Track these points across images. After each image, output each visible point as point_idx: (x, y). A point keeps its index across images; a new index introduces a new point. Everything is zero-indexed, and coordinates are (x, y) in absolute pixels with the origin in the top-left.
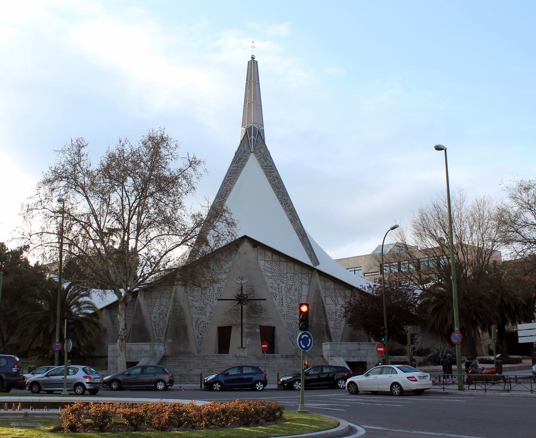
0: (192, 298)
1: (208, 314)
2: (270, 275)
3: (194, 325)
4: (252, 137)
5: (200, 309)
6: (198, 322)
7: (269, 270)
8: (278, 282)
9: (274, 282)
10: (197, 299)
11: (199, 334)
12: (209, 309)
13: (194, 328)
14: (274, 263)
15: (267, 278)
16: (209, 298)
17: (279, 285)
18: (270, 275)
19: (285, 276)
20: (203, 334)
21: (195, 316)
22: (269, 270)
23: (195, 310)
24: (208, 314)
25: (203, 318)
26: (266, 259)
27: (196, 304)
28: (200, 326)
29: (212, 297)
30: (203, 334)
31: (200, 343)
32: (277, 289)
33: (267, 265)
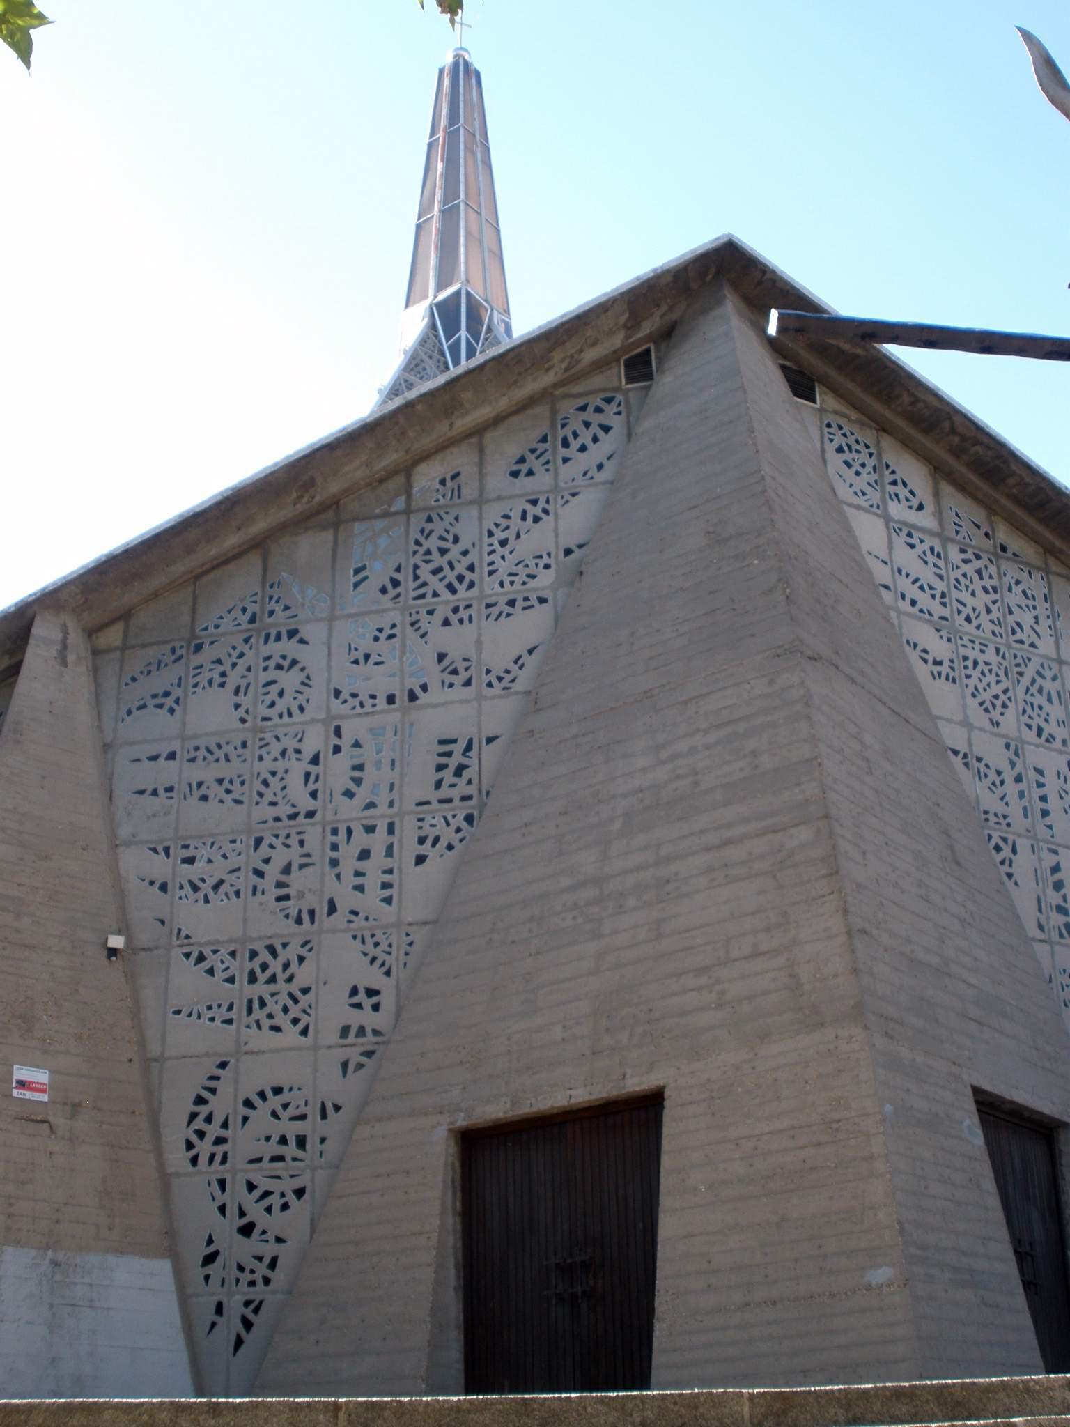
0: (160, 867)
1: (331, 1010)
2: (939, 648)
3: (176, 1132)
4: (463, 333)
5: (240, 967)
6: (220, 1105)
7: (924, 600)
8: (1010, 721)
9: (979, 718)
10: (219, 870)
11: (225, 1229)
12: (338, 962)
13: (177, 1158)
14: (954, 555)
15: (922, 672)
16: (348, 855)
17: (1015, 749)
18: (939, 648)
19: (1048, 685)
20: (274, 1223)
21: (190, 1041)
22: (924, 600)
23: (188, 982)
24: (331, 1010)
25: (274, 1057)
26: (896, 510)
27: (206, 921)
28: (244, 1143)
29: (378, 842)
30: (274, 1223)
31: (231, 1325)
32: (1011, 788)
33: (906, 558)
